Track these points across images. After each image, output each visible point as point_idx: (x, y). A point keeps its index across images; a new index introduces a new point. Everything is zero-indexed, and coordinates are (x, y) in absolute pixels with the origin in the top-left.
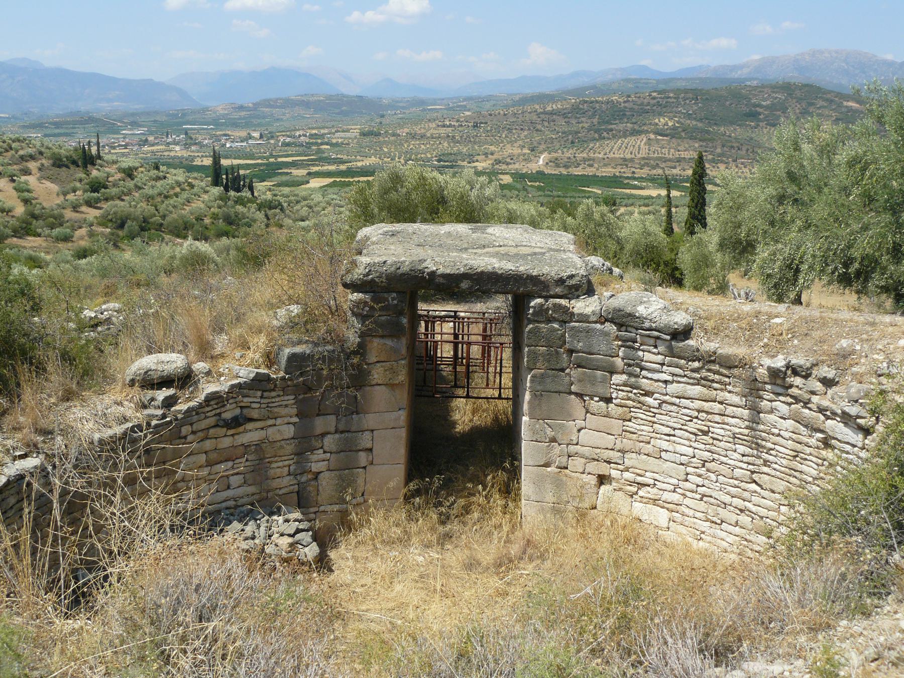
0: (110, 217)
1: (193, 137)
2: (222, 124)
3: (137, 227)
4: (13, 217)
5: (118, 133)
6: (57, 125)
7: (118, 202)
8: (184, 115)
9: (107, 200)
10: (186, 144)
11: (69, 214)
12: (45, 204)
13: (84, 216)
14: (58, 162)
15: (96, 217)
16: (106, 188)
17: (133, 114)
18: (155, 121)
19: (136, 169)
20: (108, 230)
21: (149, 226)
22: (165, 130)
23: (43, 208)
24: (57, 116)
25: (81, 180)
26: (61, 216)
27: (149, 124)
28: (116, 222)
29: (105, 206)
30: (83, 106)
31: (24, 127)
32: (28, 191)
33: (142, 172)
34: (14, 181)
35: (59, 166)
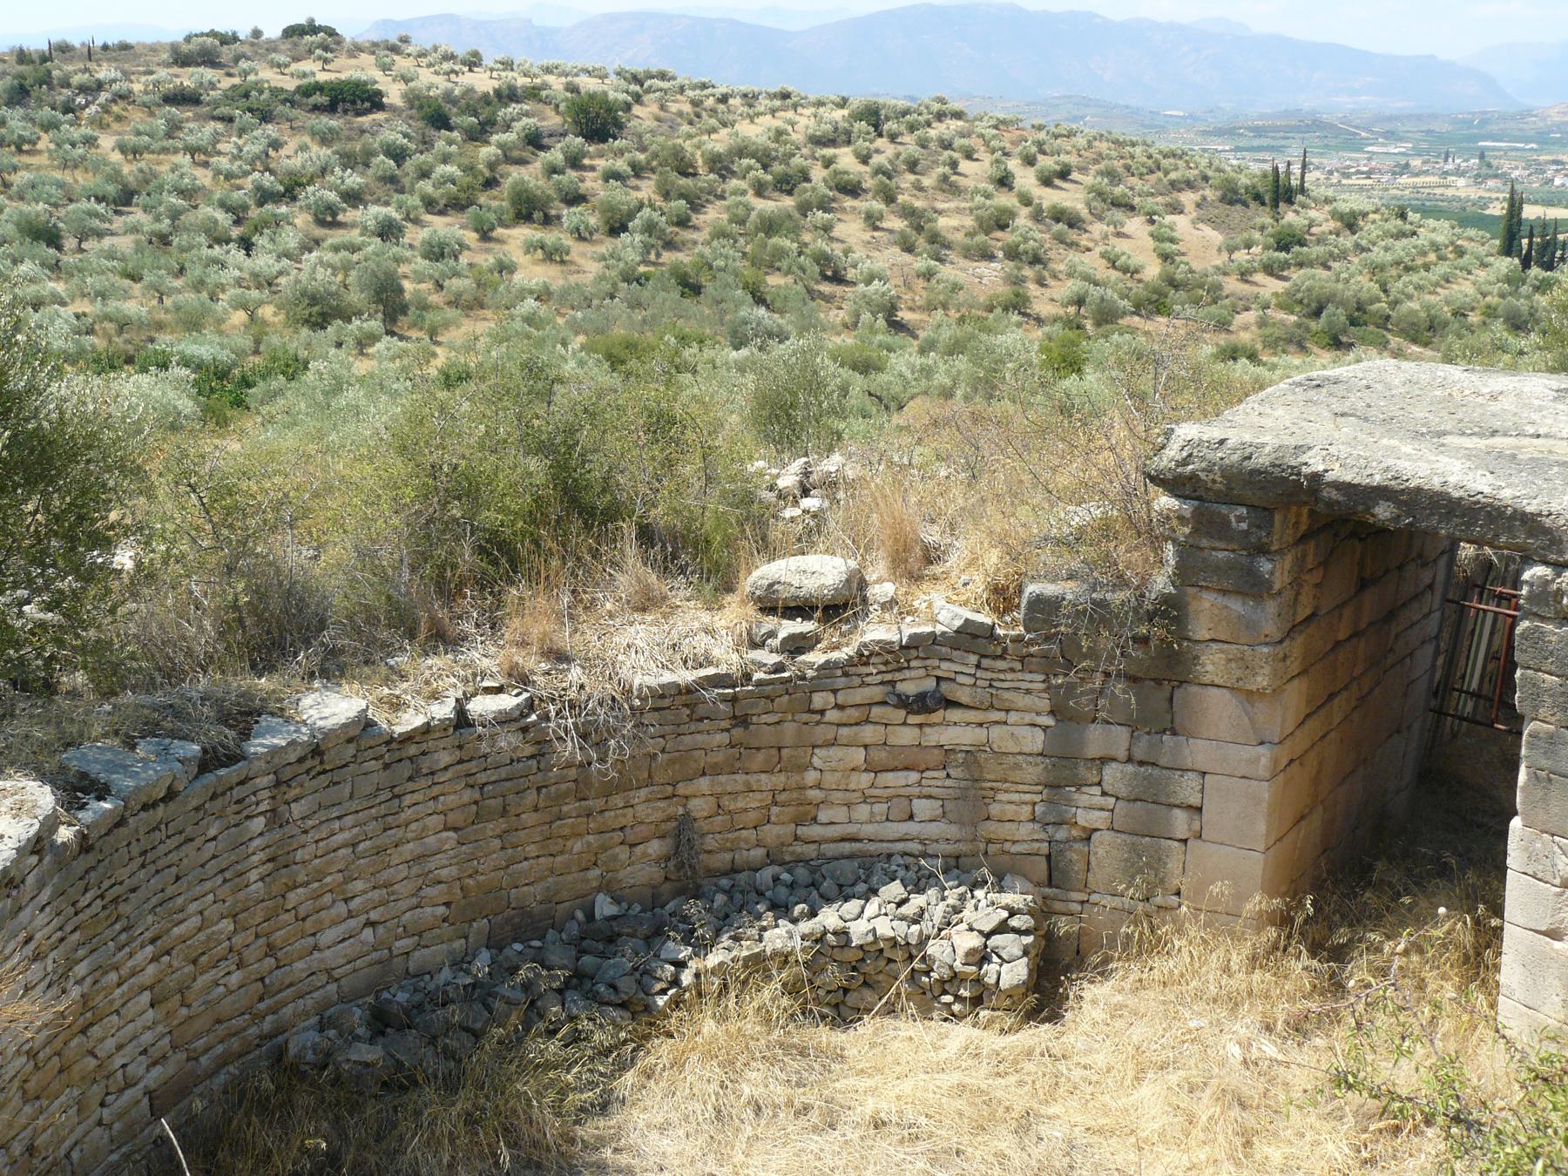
0: (1299, 296)
1: (1495, 163)
2: (1556, 142)
3: (1343, 318)
4: (1140, 281)
5: (1360, 150)
6: (1259, 131)
7: (1321, 273)
8: (1484, 122)
9: (1301, 265)
10: (1478, 175)
11: (1232, 285)
12: (1195, 265)
13: (1255, 289)
14: (1232, 196)
15: (1276, 294)
16: (1302, 245)
17: (1391, 118)
18: (1429, 132)
19: (1365, 215)
20: (1293, 318)
21: (1365, 317)
22: (1444, 149)
23: (1191, 271)
24: (1261, 117)
25: (1262, 228)
26: (1219, 287)
27: (1417, 136)
28: (1308, 305)
29: (1296, 275)
30: (1308, 101)
31: (1205, 133)
32: (1172, 240)
33: (1374, 222)
34: (1152, 222)
35: (1231, 203)
